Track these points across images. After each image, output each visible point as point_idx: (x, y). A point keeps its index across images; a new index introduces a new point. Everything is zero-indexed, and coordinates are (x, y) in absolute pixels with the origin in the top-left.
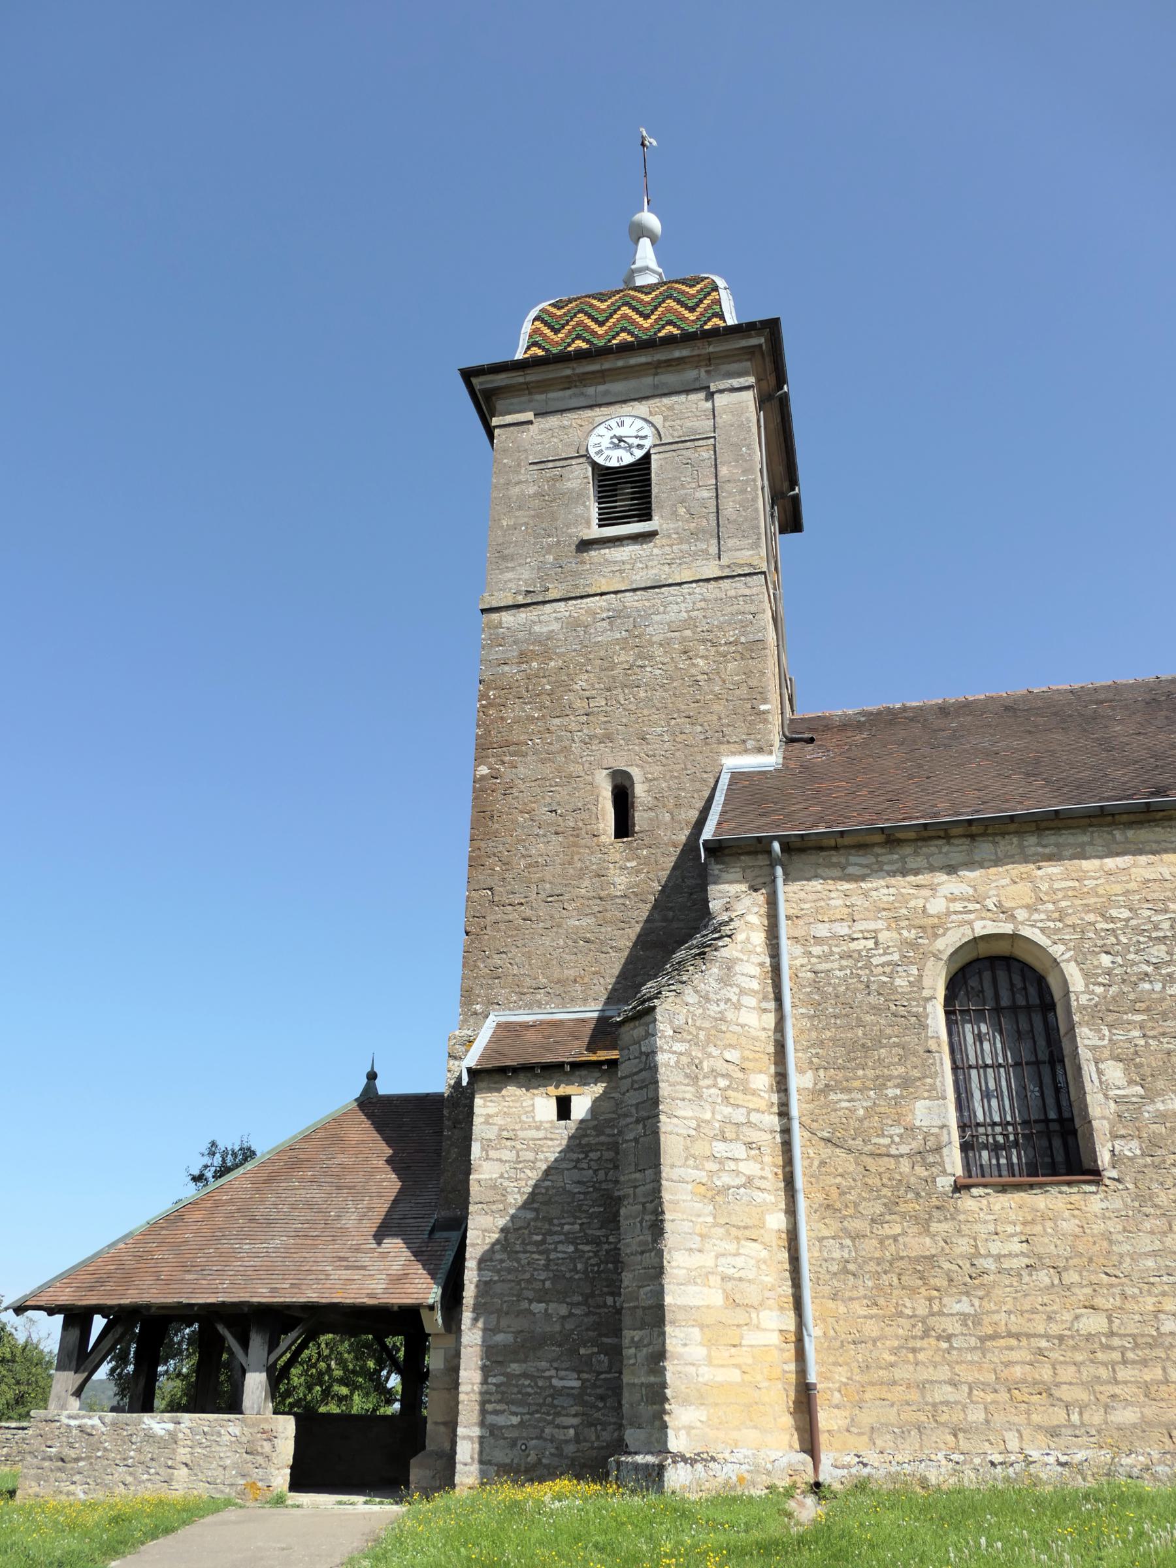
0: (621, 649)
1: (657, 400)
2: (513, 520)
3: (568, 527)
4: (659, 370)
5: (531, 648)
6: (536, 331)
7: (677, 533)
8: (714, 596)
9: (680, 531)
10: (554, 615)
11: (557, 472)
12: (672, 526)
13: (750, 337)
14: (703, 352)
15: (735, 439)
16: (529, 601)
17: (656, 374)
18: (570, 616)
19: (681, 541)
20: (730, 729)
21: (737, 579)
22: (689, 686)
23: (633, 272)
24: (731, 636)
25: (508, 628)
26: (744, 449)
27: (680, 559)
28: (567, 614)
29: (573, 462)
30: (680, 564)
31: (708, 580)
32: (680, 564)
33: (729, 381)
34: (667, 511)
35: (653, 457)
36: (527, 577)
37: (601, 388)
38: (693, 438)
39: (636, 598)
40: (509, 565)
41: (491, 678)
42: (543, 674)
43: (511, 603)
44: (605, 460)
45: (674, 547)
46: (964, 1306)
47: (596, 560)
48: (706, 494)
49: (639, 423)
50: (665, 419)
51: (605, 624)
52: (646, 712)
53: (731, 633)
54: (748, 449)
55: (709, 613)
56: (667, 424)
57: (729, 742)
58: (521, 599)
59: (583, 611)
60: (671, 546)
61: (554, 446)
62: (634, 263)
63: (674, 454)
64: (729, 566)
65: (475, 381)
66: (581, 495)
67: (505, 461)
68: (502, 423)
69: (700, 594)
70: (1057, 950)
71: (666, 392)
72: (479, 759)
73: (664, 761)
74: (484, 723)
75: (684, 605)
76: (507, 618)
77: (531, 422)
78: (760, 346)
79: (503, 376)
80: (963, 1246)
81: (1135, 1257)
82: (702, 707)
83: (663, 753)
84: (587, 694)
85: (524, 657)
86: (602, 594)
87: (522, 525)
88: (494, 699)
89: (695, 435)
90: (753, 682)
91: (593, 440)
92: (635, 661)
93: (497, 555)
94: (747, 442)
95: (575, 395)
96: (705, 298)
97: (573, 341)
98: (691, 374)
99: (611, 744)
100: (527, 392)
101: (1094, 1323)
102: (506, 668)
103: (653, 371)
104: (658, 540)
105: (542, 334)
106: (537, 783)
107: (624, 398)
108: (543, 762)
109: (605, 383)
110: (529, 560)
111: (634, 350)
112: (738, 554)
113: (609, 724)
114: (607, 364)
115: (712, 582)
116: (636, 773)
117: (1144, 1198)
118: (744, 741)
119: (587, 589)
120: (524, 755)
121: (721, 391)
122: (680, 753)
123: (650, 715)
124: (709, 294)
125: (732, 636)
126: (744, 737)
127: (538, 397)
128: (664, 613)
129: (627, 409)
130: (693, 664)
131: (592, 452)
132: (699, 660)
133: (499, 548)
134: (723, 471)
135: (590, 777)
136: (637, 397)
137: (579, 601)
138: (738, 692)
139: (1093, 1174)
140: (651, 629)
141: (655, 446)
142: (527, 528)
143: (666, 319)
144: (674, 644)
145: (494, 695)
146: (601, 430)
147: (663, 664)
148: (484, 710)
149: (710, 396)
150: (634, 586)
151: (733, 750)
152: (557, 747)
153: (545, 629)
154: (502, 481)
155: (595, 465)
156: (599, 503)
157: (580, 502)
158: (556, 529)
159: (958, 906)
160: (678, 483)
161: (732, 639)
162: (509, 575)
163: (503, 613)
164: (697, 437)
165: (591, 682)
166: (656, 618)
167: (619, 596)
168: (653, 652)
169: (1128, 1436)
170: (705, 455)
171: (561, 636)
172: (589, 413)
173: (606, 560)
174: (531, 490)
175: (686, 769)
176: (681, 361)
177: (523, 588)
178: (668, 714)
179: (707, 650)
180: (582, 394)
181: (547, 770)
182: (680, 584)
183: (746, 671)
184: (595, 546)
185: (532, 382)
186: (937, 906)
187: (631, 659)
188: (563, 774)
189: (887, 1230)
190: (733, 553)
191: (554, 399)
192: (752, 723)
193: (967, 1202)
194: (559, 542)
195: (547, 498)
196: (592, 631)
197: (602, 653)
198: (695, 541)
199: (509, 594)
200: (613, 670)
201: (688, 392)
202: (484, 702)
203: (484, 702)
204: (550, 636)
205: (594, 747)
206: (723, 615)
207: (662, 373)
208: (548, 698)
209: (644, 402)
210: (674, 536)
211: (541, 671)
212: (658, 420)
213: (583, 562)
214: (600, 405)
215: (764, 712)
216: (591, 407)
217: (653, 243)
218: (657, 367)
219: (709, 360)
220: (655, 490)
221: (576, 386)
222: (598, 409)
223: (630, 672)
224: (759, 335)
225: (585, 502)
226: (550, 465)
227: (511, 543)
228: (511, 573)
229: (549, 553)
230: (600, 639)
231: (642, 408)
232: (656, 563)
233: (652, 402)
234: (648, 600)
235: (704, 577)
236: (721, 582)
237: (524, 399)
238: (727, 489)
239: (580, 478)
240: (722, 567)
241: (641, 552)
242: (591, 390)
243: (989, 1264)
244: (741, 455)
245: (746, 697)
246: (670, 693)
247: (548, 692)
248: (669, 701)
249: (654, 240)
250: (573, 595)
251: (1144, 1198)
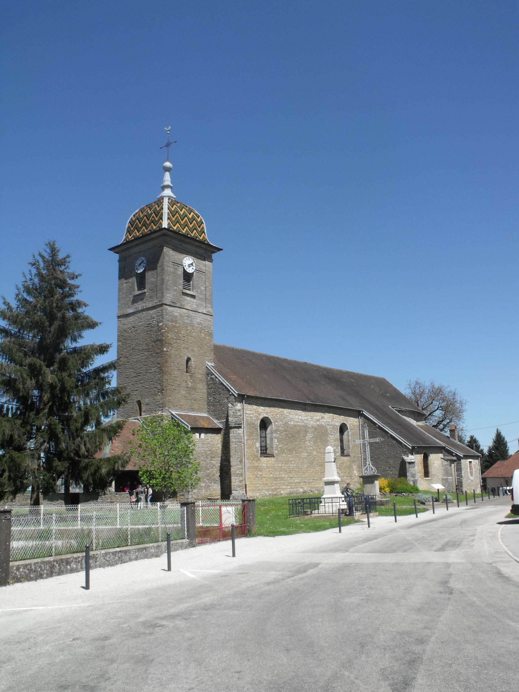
11: (176, 267)
17: (196, 248)
31: (204, 314)
37: (186, 246)
42: (174, 327)
46: (260, 473)
51: (186, 317)
70: (272, 420)
80: (260, 465)
81: (276, 467)
86: (186, 309)
101: (271, 476)
102: (168, 322)
116: (192, 359)
117: (277, 459)
120: (173, 348)
139: (272, 456)
152: (178, 348)
155: (184, 269)
159: (262, 411)
169: (273, 490)
174: (172, 270)
186: (260, 411)
189: (254, 462)
193: (261, 459)
197: (186, 326)
204: (176, 317)
212: (195, 261)
226: (176, 264)
239: (180, 272)
243: (263, 467)
251: (277, 459)
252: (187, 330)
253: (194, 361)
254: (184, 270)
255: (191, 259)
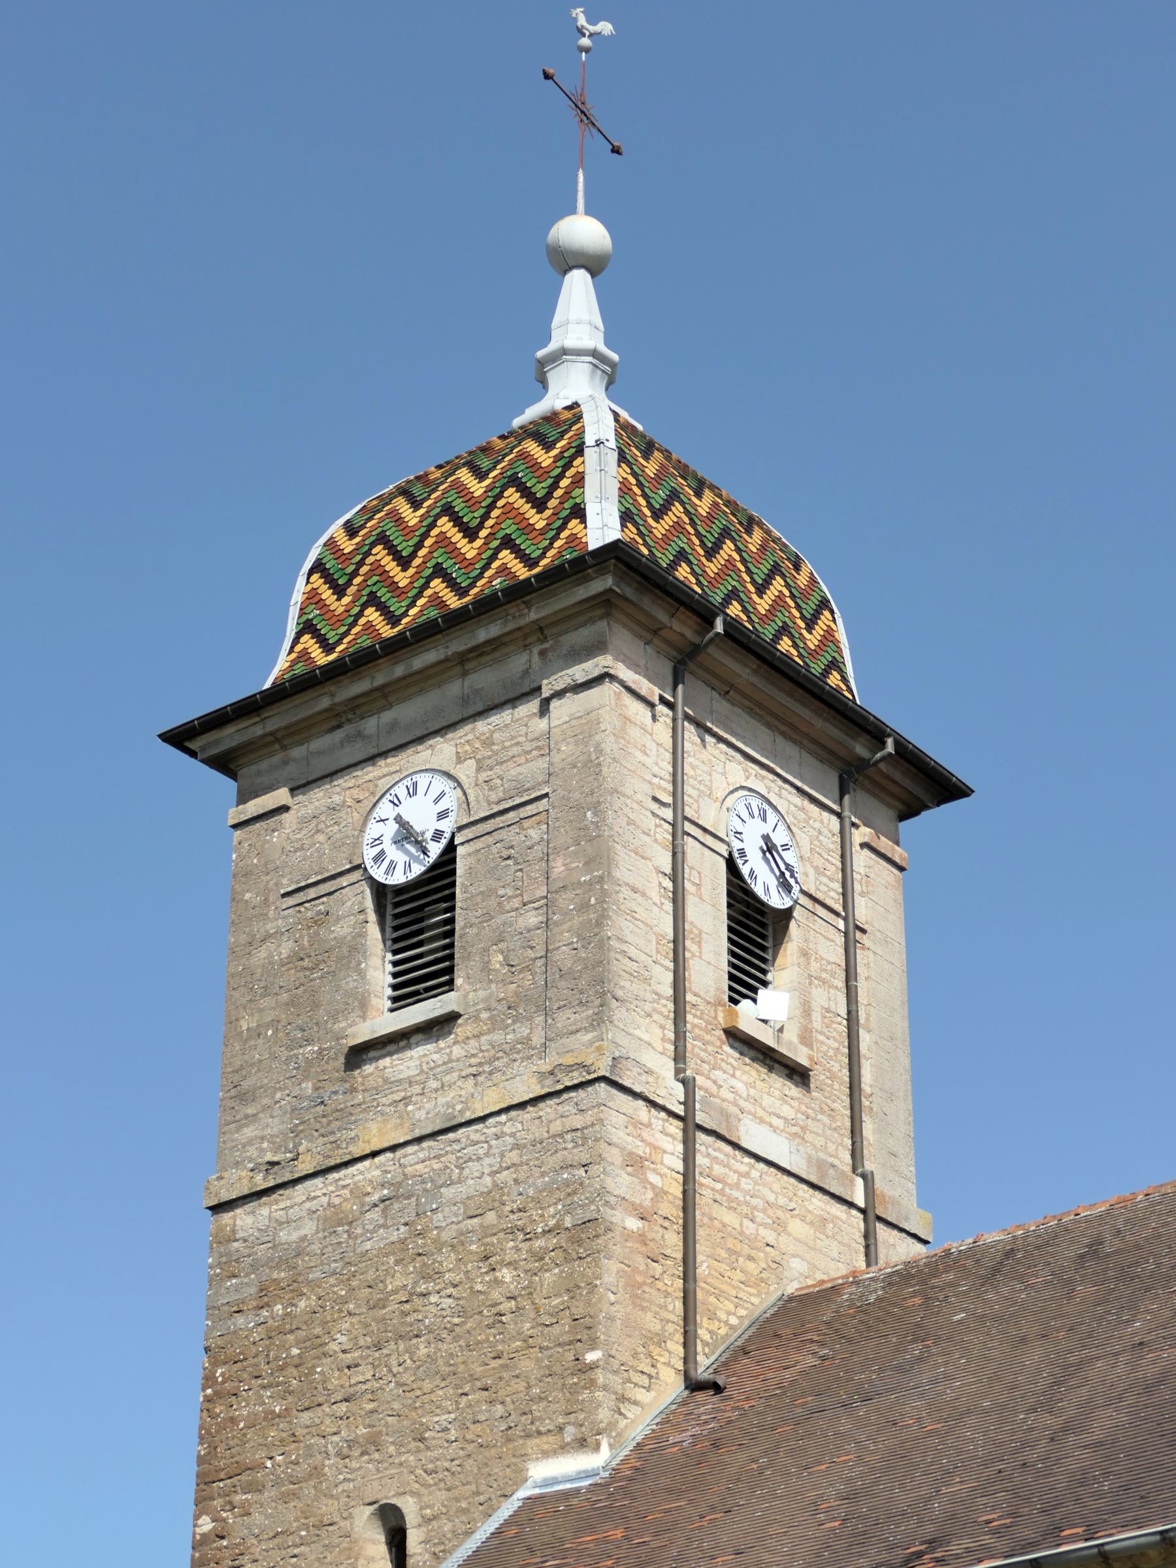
0: (397, 1262)
1: (469, 727)
2: (256, 1016)
3: (334, 1018)
4: (468, 666)
5: (275, 1275)
6: (312, 597)
7: (489, 1009)
8: (531, 1137)
9: (494, 1004)
10: (308, 1205)
12: (482, 994)
13: (588, 579)
14: (522, 622)
15: (577, 795)
16: (271, 1183)
17: (465, 674)
18: (329, 1204)
19: (496, 1024)
20: (543, 1404)
21: (565, 1096)
22: (489, 1327)
23: (542, 364)
24: (551, 1214)
25: (245, 1241)
26: (589, 814)
27: (490, 1063)
28: (325, 1200)
29: (344, 881)
30: (491, 1073)
31: (522, 1105)
32: (491, 1073)
33: (570, 671)
34: (475, 964)
35: (460, 851)
36: (275, 1130)
37: (387, 716)
38: (518, 801)
39: (421, 1155)
40: (250, 1111)
41: (220, 1342)
43: (246, 1191)
44: (387, 873)
45: (483, 1038)
47: (371, 1082)
48: (533, 919)
49: (440, 784)
50: (479, 769)
51: (375, 1215)
52: (427, 1386)
53: (552, 1210)
54: (595, 814)
55: (522, 1174)
56: (483, 776)
57: (539, 1433)
58: (261, 1182)
59: (347, 1191)
60: (477, 1037)
61: (318, 850)
62: (548, 339)
63: (489, 839)
64: (552, 1073)
65: (193, 745)
66: (355, 948)
67: (248, 896)
68: (243, 818)
69: (513, 1135)
71: (480, 708)
72: (202, 1503)
73: (450, 1480)
74: (208, 1432)
75: (487, 1161)
76: (243, 1220)
77: (285, 809)
78: (610, 590)
79: (230, 730)
82: (505, 1367)
83: (447, 1464)
84: (348, 1358)
85: (265, 1295)
86: (374, 1154)
87: (268, 1026)
88: (223, 1382)
89: (519, 794)
90: (578, 1312)
91: (374, 830)
92: (416, 1283)
93: (233, 1092)
94: (595, 800)
95: (349, 739)
96: (561, 476)
97: (360, 614)
98: (518, 662)
99: (377, 1456)
100: (277, 746)
102: (240, 1320)
103: (458, 670)
104: (462, 1029)
105: (320, 603)
106: (276, 1541)
107: (419, 734)
108: (285, 1498)
109: (390, 706)
110: (278, 1095)
111: (410, 644)
112: (571, 1042)
113: (375, 1416)
114: (380, 676)
115: (530, 1108)
118: (561, 1429)
119: (351, 1148)
121: (559, 694)
122: (471, 1461)
123: (432, 1392)
124: (568, 466)
125: (554, 1217)
126: (561, 1420)
127: (297, 752)
128: (459, 1181)
129: (422, 755)
130: (497, 1282)
131: (369, 854)
132: (505, 1270)
133: (236, 1078)
134: (558, 867)
135: (347, 1523)
136: (438, 727)
137: (343, 1173)
138: (556, 1330)
140: (440, 1215)
141: (460, 828)
142: (276, 1031)
143: (501, 534)
144: (472, 1243)
145: (222, 1374)
146: (385, 809)
147: (455, 1286)
148: (210, 1406)
149: (544, 709)
150: (418, 1133)
151: (546, 1447)
153: (295, 1236)
154: (243, 938)
156: (395, 953)
157: (353, 964)
158: (317, 1024)
160: (493, 902)
161: (552, 1223)
162: (249, 1132)
163: (239, 1211)
164: (526, 798)
165: (355, 1332)
166: (448, 1192)
167: (399, 1153)
168: (441, 1263)
170: (534, 834)
171: (316, 1248)
172: (369, 773)
173: (386, 1081)
174: (286, 948)
175: (478, 1493)
176: (495, 644)
177: (269, 1157)
178: (457, 1387)
179: (518, 1249)
180: (360, 735)
181: (290, 1515)
182: (483, 1119)
183: (570, 1286)
184: (372, 1054)
185: (278, 730)
187: (409, 1281)
188: (311, 1521)
190: (564, 1040)
191: (320, 753)
192: (574, 1390)
194: (321, 1050)
195: (306, 963)
196: (359, 1231)
197: (370, 1275)
198: (514, 1022)
199: (244, 1173)
200: (384, 1307)
201: (513, 701)
202: (209, 1391)
203: (209, 1391)
205: (355, 1465)
206: (543, 1174)
207: (475, 670)
208: (295, 1373)
209: (450, 736)
210: (485, 1015)
211: (288, 1320)
212: (465, 773)
213: (353, 1090)
214: (384, 754)
215: (593, 1367)
216: (371, 759)
217: (593, 274)
218: (463, 662)
219: (540, 630)
220: (459, 925)
221: (349, 721)
222: (382, 763)
223: (407, 1306)
224: (602, 573)
225: (359, 963)
226: (312, 893)
227: (253, 1065)
228: (251, 1128)
229: (306, 1078)
230: (368, 1245)
231: (441, 751)
232: (455, 1075)
233: (461, 732)
234: (437, 1157)
235: (515, 1102)
236: (542, 1105)
237: (277, 759)
238: (567, 901)
240: (542, 1076)
241: (435, 1057)
242: (370, 725)
244: (586, 828)
245: (566, 1338)
246: (462, 1343)
247: (296, 1361)
248: (460, 1360)
249: (594, 265)
250: (332, 1162)
252: (381, 1304)
253: (427, 1520)
254: (380, 891)
255: (423, 780)
